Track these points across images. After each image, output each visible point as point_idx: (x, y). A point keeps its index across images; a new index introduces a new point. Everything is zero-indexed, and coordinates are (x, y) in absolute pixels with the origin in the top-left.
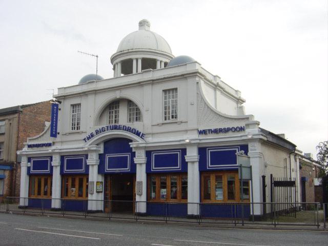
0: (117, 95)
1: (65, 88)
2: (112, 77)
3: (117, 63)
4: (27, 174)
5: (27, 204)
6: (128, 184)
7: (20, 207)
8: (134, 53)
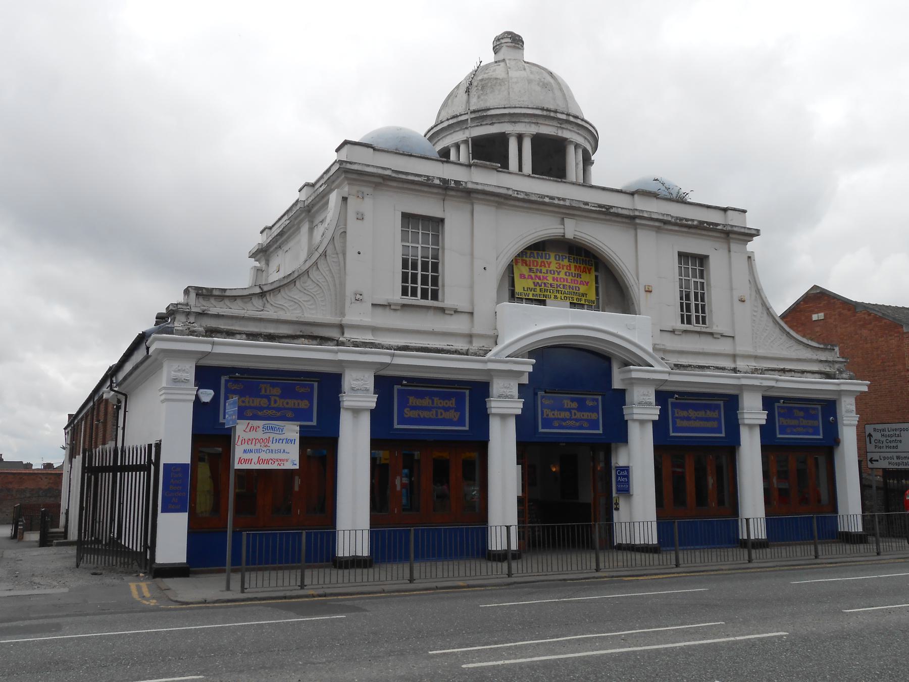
0: (572, 230)
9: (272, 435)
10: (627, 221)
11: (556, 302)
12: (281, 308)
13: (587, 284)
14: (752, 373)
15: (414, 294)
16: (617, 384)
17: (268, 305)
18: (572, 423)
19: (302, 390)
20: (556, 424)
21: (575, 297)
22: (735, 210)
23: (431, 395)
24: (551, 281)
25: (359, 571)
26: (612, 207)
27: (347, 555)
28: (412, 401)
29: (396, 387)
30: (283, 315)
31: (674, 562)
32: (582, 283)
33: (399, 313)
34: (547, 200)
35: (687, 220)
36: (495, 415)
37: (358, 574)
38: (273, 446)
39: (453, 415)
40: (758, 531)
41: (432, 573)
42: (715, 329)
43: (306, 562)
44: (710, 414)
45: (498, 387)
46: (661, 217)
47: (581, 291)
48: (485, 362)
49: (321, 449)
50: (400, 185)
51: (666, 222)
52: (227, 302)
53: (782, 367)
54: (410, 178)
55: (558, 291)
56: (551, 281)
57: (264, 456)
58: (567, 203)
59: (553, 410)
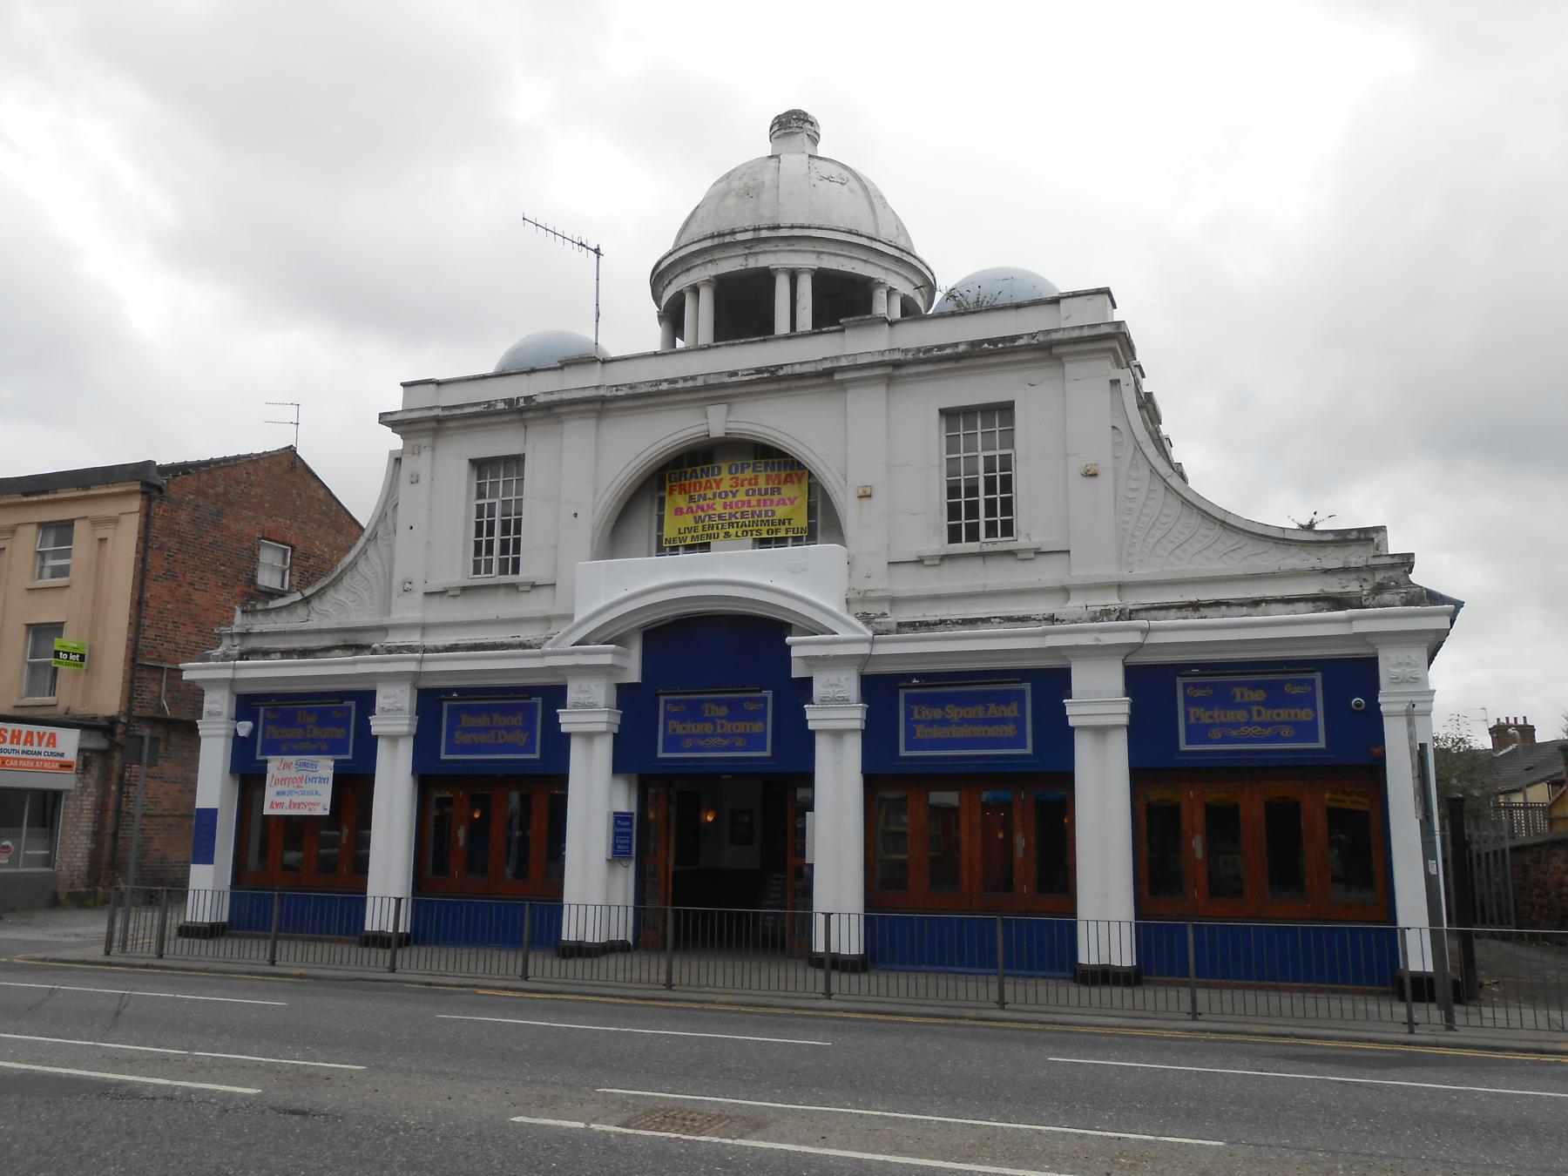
0: (717, 422)
1: (439, 383)
2: (657, 348)
3: (695, 290)
4: (232, 772)
5: (225, 919)
6: (710, 818)
7: (188, 931)
8: (783, 246)
9: (305, 773)
10: (821, 381)
11: (727, 542)
12: (325, 614)
13: (792, 502)
14: (1093, 620)
15: (489, 570)
16: (797, 672)
17: (313, 615)
18: (1250, 731)
19: (1297, 690)
20: (1216, 734)
21: (764, 529)
22: (1075, 295)
23: (488, 710)
24: (719, 509)
25: (580, 962)
26: (781, 367)
27: (1094, 961)
28: (466, 720)
29: (1180, 682)
30: (327, 624)
31: (519, 971)
32: (782, 502)
33: (460, 600)
34: (665, 386)
35: (940, 348)
36: (822, 731)
37: (840, 981)
38: (308, 787)
39: (520, 737)
40: (849, 940)
41: (296, 956)
42: (1021, 541)
43: (1198, 976)
44: (995, 711)
45: (1082, 679)
46: (877, 358)
47: (778, 516)
48: (543, 655)
49: (354, 789)
50: (462, 423)
51: (897, 365)
52: (273, 615)
53: (1194, 599)
54: (466, 410)
55: (731, 525)
56: (719, 509)
57: (297, 799)
58: (700, 382)
59: (684, 721)
